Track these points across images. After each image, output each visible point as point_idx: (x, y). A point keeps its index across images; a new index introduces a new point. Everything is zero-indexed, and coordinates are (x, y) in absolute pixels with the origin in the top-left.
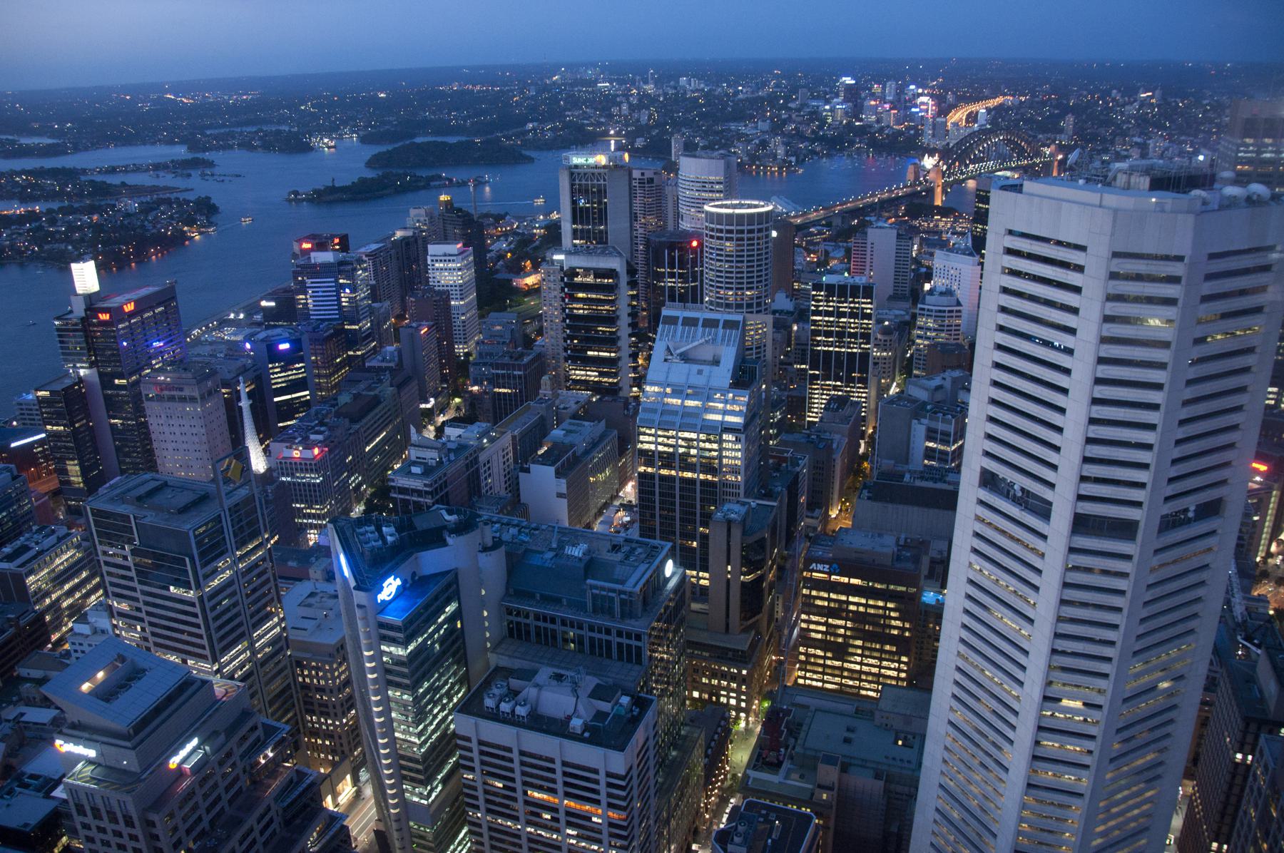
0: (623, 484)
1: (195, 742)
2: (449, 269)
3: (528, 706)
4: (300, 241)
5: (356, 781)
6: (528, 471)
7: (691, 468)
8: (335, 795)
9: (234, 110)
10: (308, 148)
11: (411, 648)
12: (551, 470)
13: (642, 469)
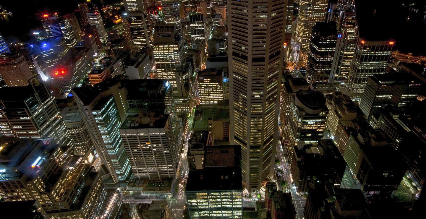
0: (152, 67)
3: (139, 124)
6: (127, 68)
7: (168, 61)
11: (104, 117)
12: (134, 66)
13: (156, 63)
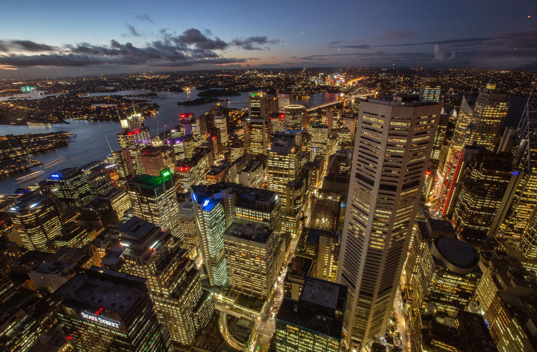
1: (157, 242)
2: (220, 123)
4: (181, 115)
5: (197, 252)
8: (192, 255)
9: (163, 80)
10: (182, 91)
